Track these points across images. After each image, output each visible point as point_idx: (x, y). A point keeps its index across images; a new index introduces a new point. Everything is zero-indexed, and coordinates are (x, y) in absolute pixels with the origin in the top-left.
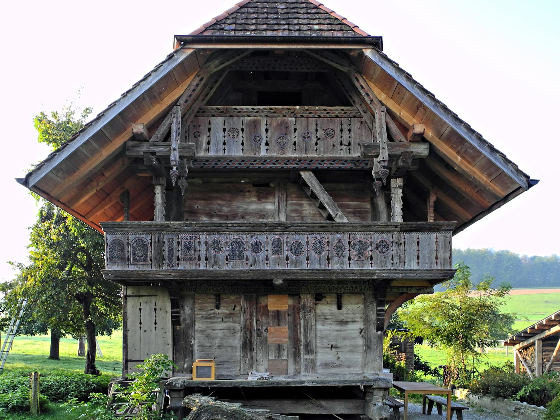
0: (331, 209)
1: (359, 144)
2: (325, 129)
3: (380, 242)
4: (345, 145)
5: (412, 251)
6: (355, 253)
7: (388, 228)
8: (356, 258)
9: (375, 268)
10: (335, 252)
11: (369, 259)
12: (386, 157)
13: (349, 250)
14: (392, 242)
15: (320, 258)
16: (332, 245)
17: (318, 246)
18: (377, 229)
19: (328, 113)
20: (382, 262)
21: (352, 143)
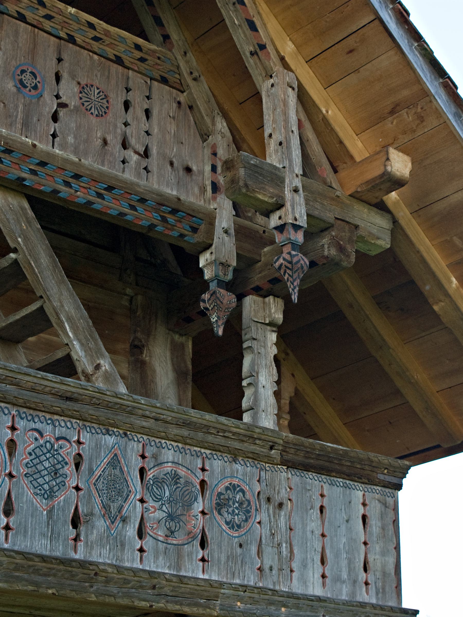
0: (80, 341)
1: (172, 164)
2: (83, 83)
3: (227, 488)
4: (136, 152)
5: (309, 534)
6: (159, 515)
7: (253, 448)
8: (161, 533)
9: (215, 577)
10: (98, 500)
11: (197, 543)
12: (301, 216)
13: (142, 501)
14: (259, 493)
15: (50, 512)
16: (91, 472)
17: (47, 464)
18: (222, 441)
19: (96, 39)
20: (231, 557)
21: (154, 151)
